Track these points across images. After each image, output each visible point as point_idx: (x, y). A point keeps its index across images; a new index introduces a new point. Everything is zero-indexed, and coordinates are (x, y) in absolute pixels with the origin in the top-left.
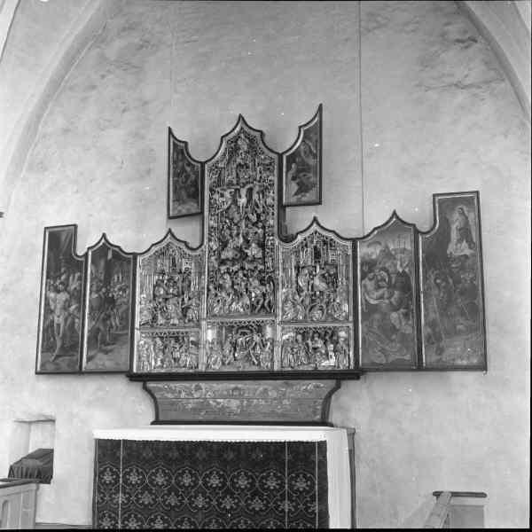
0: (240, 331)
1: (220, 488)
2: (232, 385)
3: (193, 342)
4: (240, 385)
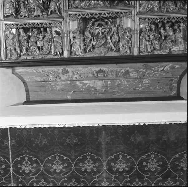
0: (97, 23)
1: (128, 172)
2: (96, 68)
3: (58, 33)
4: (104, 68)
